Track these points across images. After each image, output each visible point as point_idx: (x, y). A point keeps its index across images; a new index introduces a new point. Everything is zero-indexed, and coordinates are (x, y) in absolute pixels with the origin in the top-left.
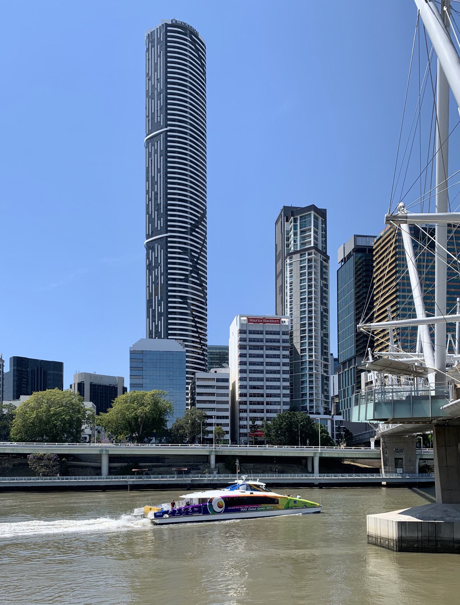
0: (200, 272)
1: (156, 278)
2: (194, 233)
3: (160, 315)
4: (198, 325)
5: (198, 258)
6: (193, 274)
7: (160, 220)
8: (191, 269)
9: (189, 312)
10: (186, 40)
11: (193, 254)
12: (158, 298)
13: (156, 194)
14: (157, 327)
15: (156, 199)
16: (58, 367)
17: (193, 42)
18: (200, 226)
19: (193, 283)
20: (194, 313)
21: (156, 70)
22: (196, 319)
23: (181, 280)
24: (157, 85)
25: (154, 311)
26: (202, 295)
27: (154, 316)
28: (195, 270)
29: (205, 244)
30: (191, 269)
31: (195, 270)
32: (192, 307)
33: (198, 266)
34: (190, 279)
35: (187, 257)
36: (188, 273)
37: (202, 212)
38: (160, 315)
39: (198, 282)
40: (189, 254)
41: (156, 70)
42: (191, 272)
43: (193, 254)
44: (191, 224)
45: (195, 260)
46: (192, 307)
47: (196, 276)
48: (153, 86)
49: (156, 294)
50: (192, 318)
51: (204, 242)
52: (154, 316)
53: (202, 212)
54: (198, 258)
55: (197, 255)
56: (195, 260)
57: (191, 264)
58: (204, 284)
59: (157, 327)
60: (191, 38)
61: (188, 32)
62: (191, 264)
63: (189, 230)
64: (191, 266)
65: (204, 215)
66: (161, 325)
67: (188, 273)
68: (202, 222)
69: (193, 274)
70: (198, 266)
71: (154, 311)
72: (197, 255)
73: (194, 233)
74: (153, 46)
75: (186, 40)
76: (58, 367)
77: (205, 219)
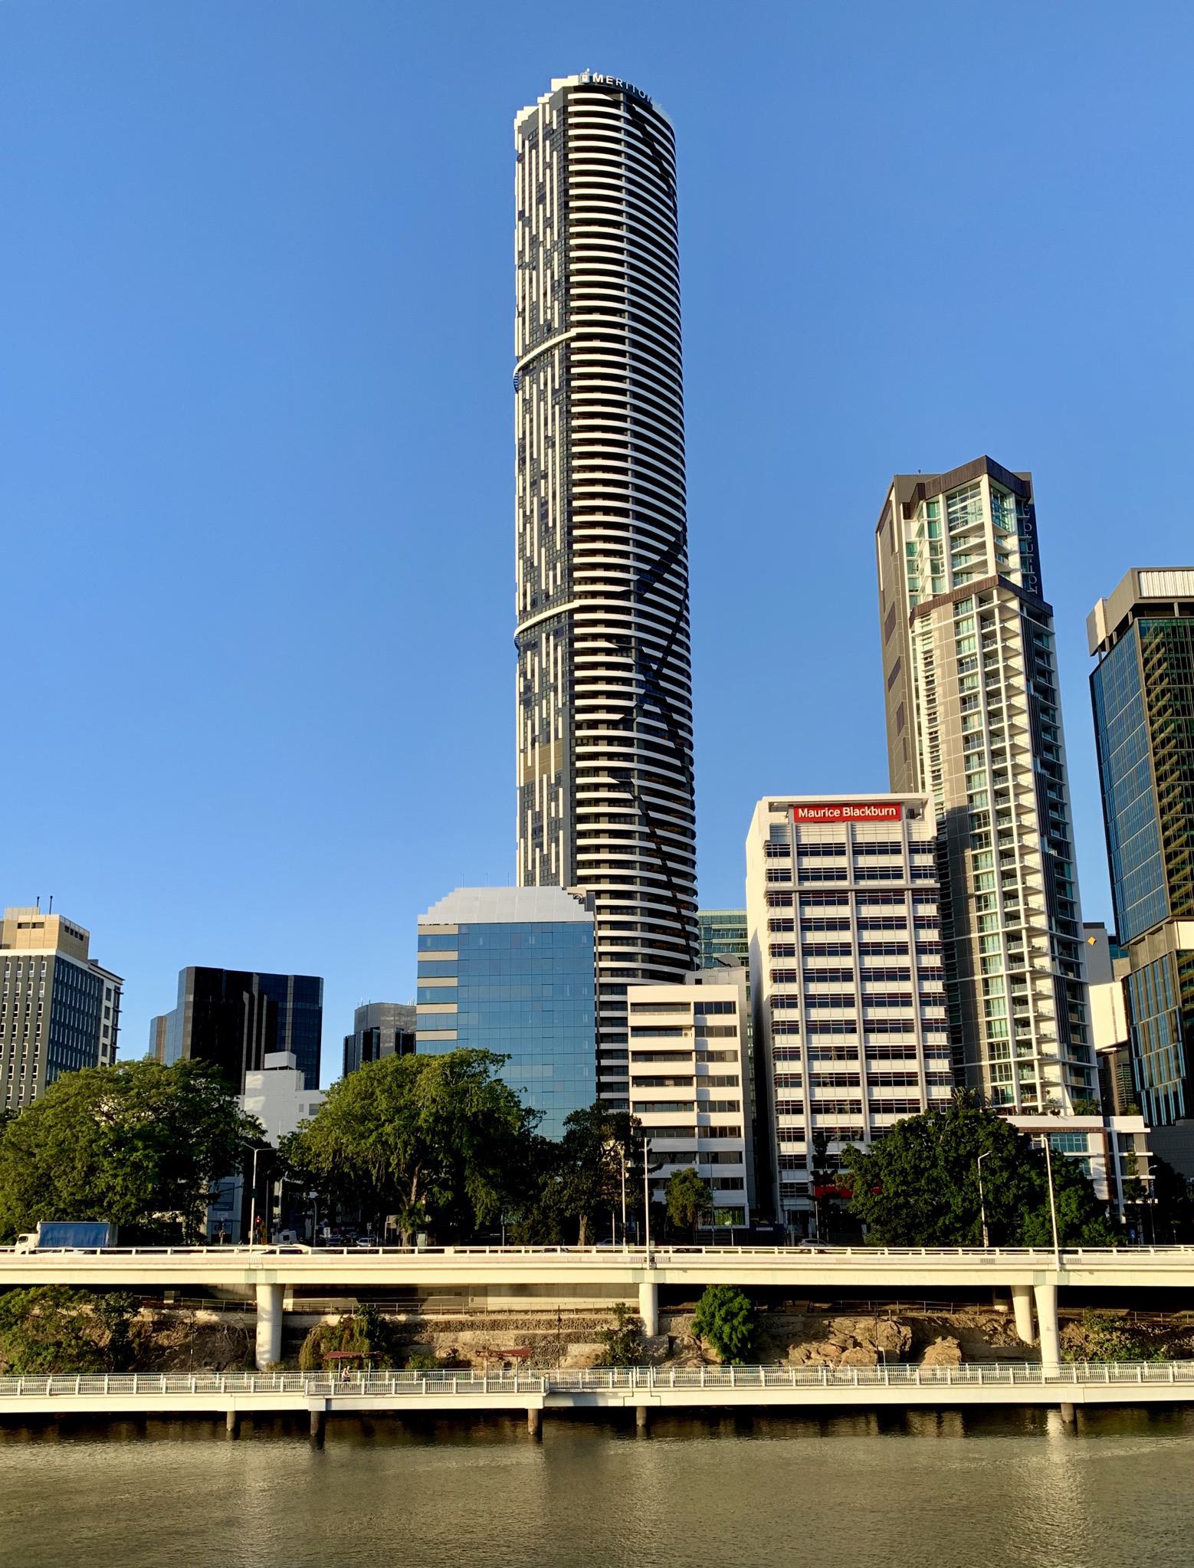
1: (545, 724)
2: (648, 595)
3: (555, 824)
6: (646, 707)
7: (555, 568)
8: (642, 691)
10: (617, 117)
12: (549, 778)
13: (543, 504)
14: (545, 860)
15: (544, 516)
16: (309, 988)
17: (637, 121)
18: (666, 576)
19: (649, 729)
20: (652, 814)
21: (541, 199)
24: (545, 233)
25: (537, 817)
26: (678, 763)
27: (537, 831)
28: (653, 693)
29: (682, 624)
30: (642, 691)
33: (663, 684)
35: (629, 661)
37: (673, 539)
38: (555, 824)
39: (664, 726)
41: (541, 199)
42: (642, 699)
44: (638, 571)
45: (655, 667)
47: (657, 710)
48: (534, 240)
49: (545, 769)
51: (680, 616)
52: (537, 831)
53: (673, 539)
54: (663, 663)
55: (660, 655)
56: (655, 667)
57: (641, 677)
58: (681, 733)
59: (545, 860)
60: (630, 110)
61: (622, 97)
62: (641, 677)
65: (678, 546)
66: (558, 853)
67: (631, 704)
68: (674, 566)
69: (646, 707)
70: (663, 684)
71: (537, 817)
72: (660, 655)
73: (648, 595)
74: (534, 146)
75: (617, 117)
76: (309, 988)
77: (680, 557)
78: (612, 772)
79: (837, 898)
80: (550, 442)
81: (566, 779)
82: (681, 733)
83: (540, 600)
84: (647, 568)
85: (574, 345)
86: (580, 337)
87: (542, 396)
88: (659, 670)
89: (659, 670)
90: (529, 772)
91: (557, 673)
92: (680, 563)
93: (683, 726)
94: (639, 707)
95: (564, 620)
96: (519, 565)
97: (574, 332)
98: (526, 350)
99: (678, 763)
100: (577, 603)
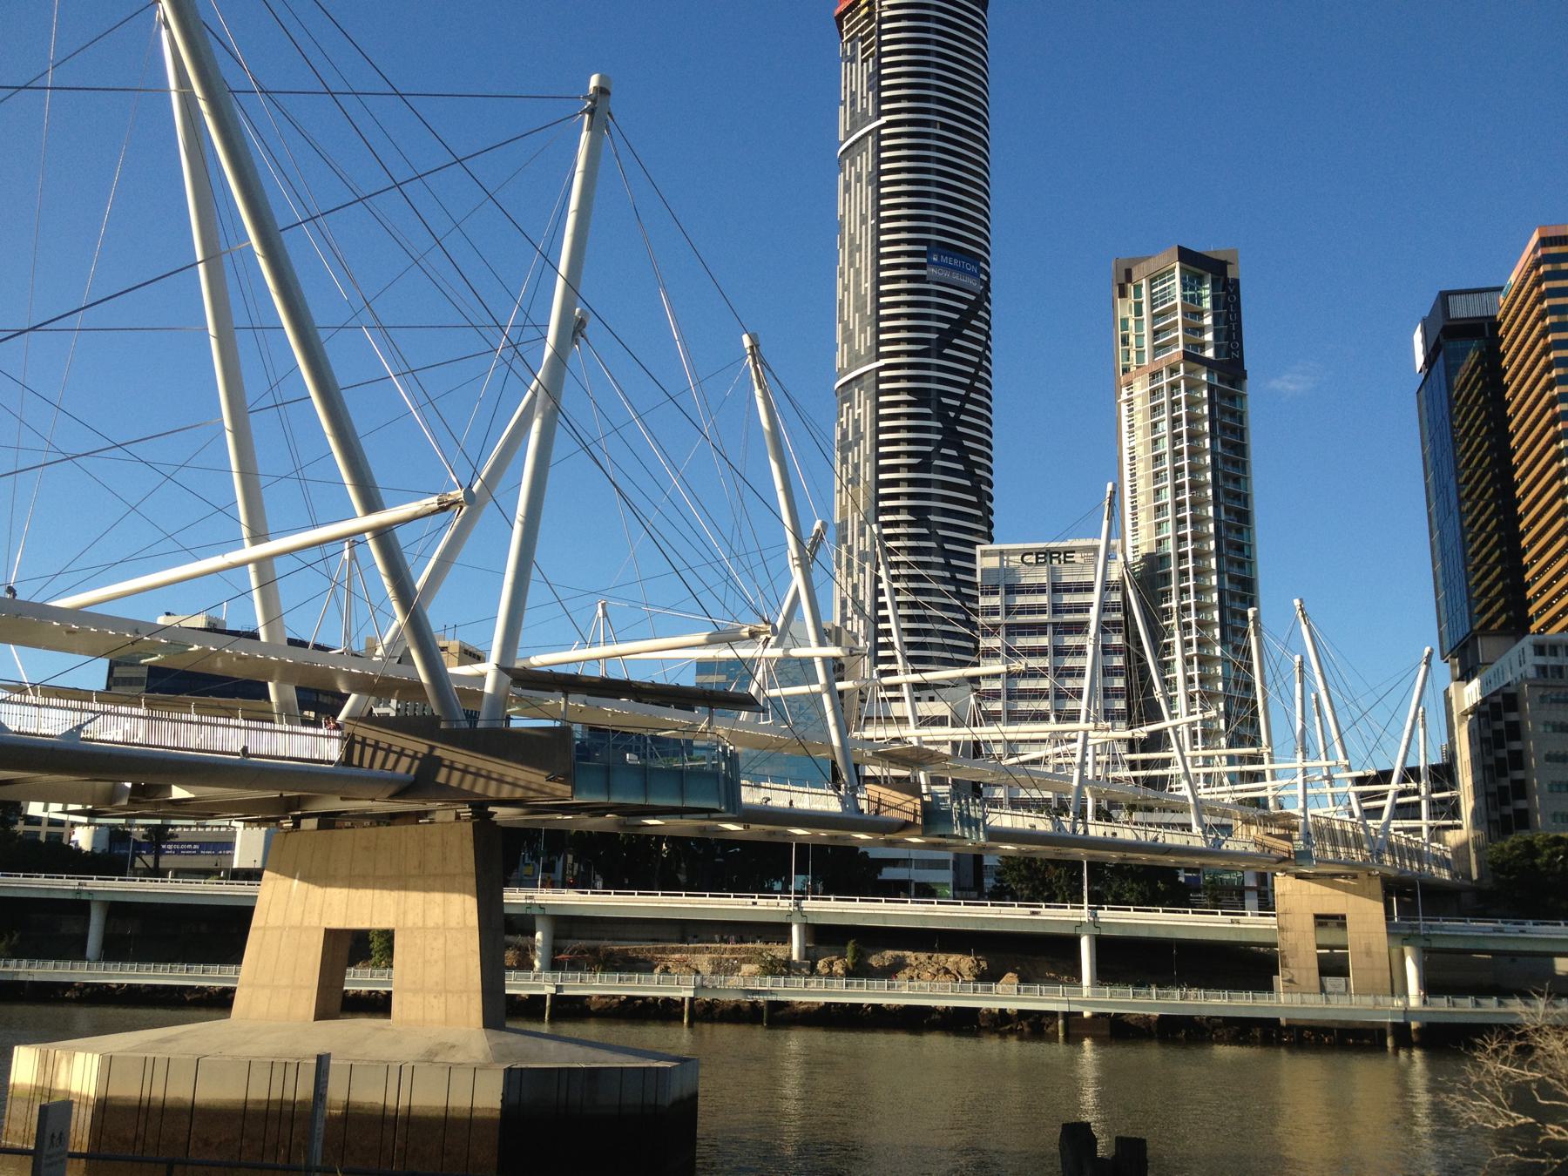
0: (966, 443)
2: (947, 351)
4: (959, 576)
5: (961, 410)
6: (943, 451)
8: (939, 437)
9: (933, 544)
11: (945, 400)
14: (855, 588)
15: (858, 285)
19: (945, 471)
20: (947, 546)
22: (954, 562)
23: (910, 468)
25: (850, 550)
26: (974, 499)
28: (951, 437)
30: (939, 437)
31: (951, 437)
32: (941, 532)
33: (960, 429)
34: (936, 462)
35: (928, 411)
36: (929, 449)
39: (961, 467)
40: (934, 403)
42: (940, 444)
43: (945, 400)
44: (939, 330)
45: (952, 414)
46: (941, 532)
47: (954, 453)
50: (942, 560)
56: (952, 414)
59: (855, 588)
63: (933, 346)
64: (938, 431)
67: (929, 449)
69: (943, 451)
70: (960, 429)
71: (850, 550)
73: (947, 351)
78: (910, 510)
79: (1040, 629)
80: (864, 221)
81: (871, 516)
82: (978, 472)
83: (855, 360)
84: (946, 326)
85: (883, 132)
86: (889, 124)
87: (859, 178)
88: (957, 418)
89: (957, 418)
90: (844, 512)
91: (867, 428)
92: (980, 319)
93: (980, 466)
94: (937, 451)
95: (871, 380)
96: (839, 327)
97: (884, 120)
98: (848, 135)
99: (974, 499)
100: (882, 362)
